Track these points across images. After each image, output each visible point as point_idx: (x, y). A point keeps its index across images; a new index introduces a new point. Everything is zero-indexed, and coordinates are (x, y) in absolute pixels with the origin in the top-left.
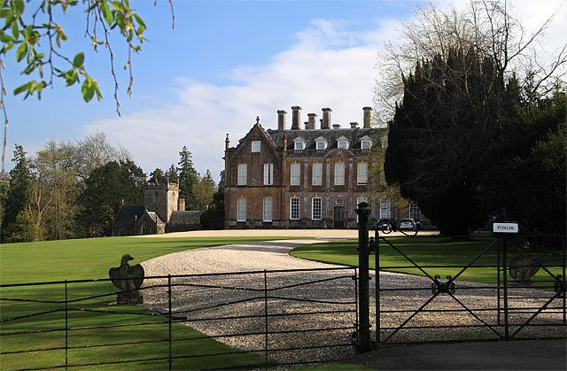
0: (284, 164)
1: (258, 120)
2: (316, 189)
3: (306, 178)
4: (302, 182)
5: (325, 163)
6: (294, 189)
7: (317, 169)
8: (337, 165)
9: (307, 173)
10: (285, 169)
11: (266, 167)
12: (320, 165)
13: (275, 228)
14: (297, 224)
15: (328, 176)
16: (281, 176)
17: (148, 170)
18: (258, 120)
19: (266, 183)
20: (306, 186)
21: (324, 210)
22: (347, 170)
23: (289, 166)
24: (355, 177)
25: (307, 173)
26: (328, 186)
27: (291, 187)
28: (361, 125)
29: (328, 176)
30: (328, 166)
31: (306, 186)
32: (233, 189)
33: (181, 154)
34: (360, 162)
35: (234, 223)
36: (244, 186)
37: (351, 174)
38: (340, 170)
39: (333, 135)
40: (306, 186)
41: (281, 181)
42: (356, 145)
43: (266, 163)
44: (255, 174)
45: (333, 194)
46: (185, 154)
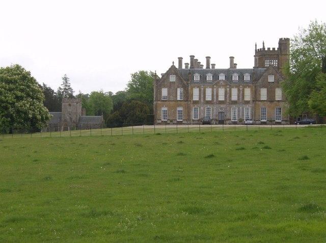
0: (190, 88)
1: (173, 63)
2: (208, 102)
3: (202, 96)
4: (200, 98)
5: (213, 88)
6: (195, 102)
7: (209, 91)
8: (220, 89)
9: (203, 94)
10: (189, 91)
11: (179, 90)
12: (211, 89)
13: (184, 124)
14: (197, 122)
15: (215, 95)
16: (187, 96)
17: (56, 91)
18: (173, 63)
19: (179, 99)
20: (203, 101)
21: (212, 114)
22: (226, 92)
23: (192, 89)
24: (230, 96)
25: (203, 94)
26: (215, 101)
27: (194, 101)
28: (177, 66)
29: (215, 95)
30: (215, 89)
31: (202, 100)
32: (159, 102)
33: (63, 79)
34: (194, 87)
35: (160, 122)
36: (264, 101)
37: (228, 94)
38: (222, 92)
39: (216, 73)
40: (202, 100)
41: (188, 98)
42: (203, 78)
43: (179, 87)
44: (172, 93)
45: (218, 106)
46: (66, 79)
